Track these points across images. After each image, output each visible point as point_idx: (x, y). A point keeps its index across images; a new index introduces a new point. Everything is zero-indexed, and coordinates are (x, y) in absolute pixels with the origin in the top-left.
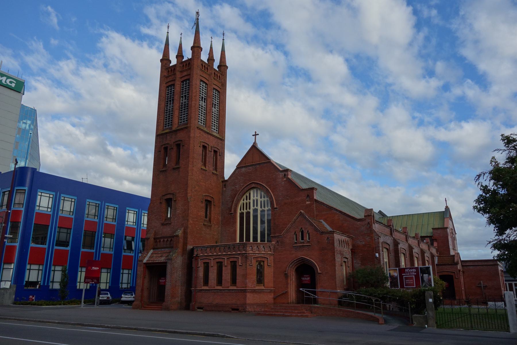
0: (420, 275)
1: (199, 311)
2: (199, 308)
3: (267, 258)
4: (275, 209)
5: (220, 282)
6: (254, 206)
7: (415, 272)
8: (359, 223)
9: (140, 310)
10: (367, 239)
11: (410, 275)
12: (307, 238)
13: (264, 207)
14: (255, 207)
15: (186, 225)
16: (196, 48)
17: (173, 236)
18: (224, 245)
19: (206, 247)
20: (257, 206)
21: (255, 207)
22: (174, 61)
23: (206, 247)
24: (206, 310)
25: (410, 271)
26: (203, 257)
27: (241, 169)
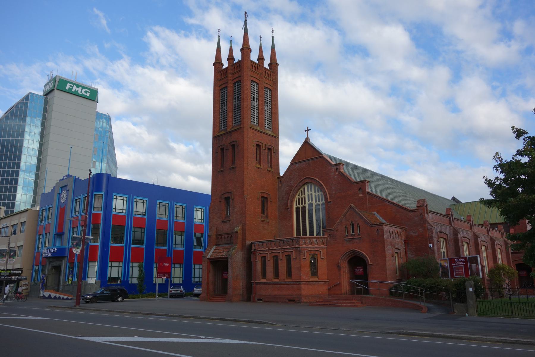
0: (469, 265)
1: (259, 302)
3: (320, 251)
4: (329, 203)
5: (276, 275)
6: (309, 201)
7: (464, 262)
8: (412, 213)
9: (207, 302)
10: (420, 229)
11: (459, 265)
12: (357, 230)
13: (319, 201)
14: (310, 201)
15: (244, 222)
16: (246, 49)
17: (233, 233)
18: (278, 240)
20: (312, 200)
21: (310, 201)
22: (226, 65)
24: (265, 301)
25: (459, 261)
26: (260, 251)
27: (295, 165)
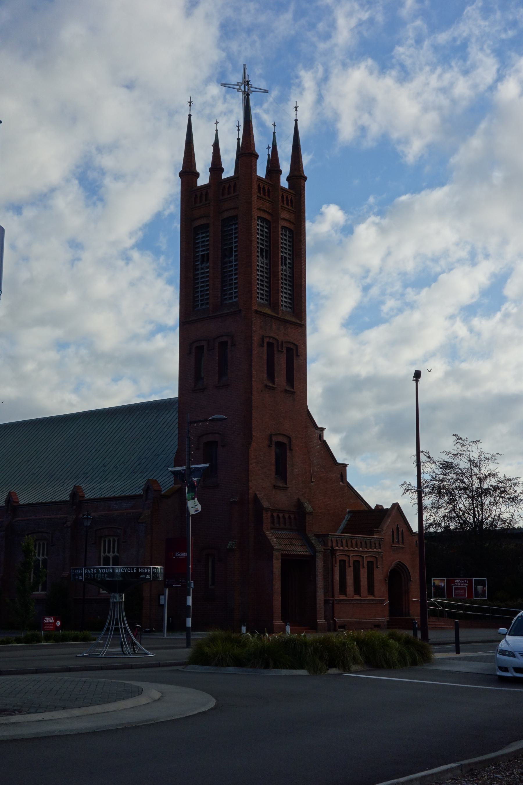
2: (340, 627)
5: (357, 590)
11: (461, 586)
19: (343, 537)
23: (343, 537)
25: (461, 582)
